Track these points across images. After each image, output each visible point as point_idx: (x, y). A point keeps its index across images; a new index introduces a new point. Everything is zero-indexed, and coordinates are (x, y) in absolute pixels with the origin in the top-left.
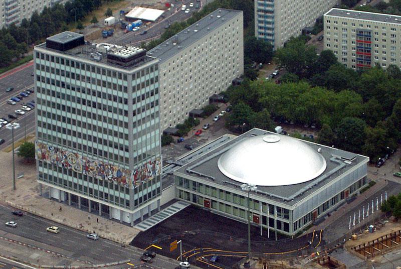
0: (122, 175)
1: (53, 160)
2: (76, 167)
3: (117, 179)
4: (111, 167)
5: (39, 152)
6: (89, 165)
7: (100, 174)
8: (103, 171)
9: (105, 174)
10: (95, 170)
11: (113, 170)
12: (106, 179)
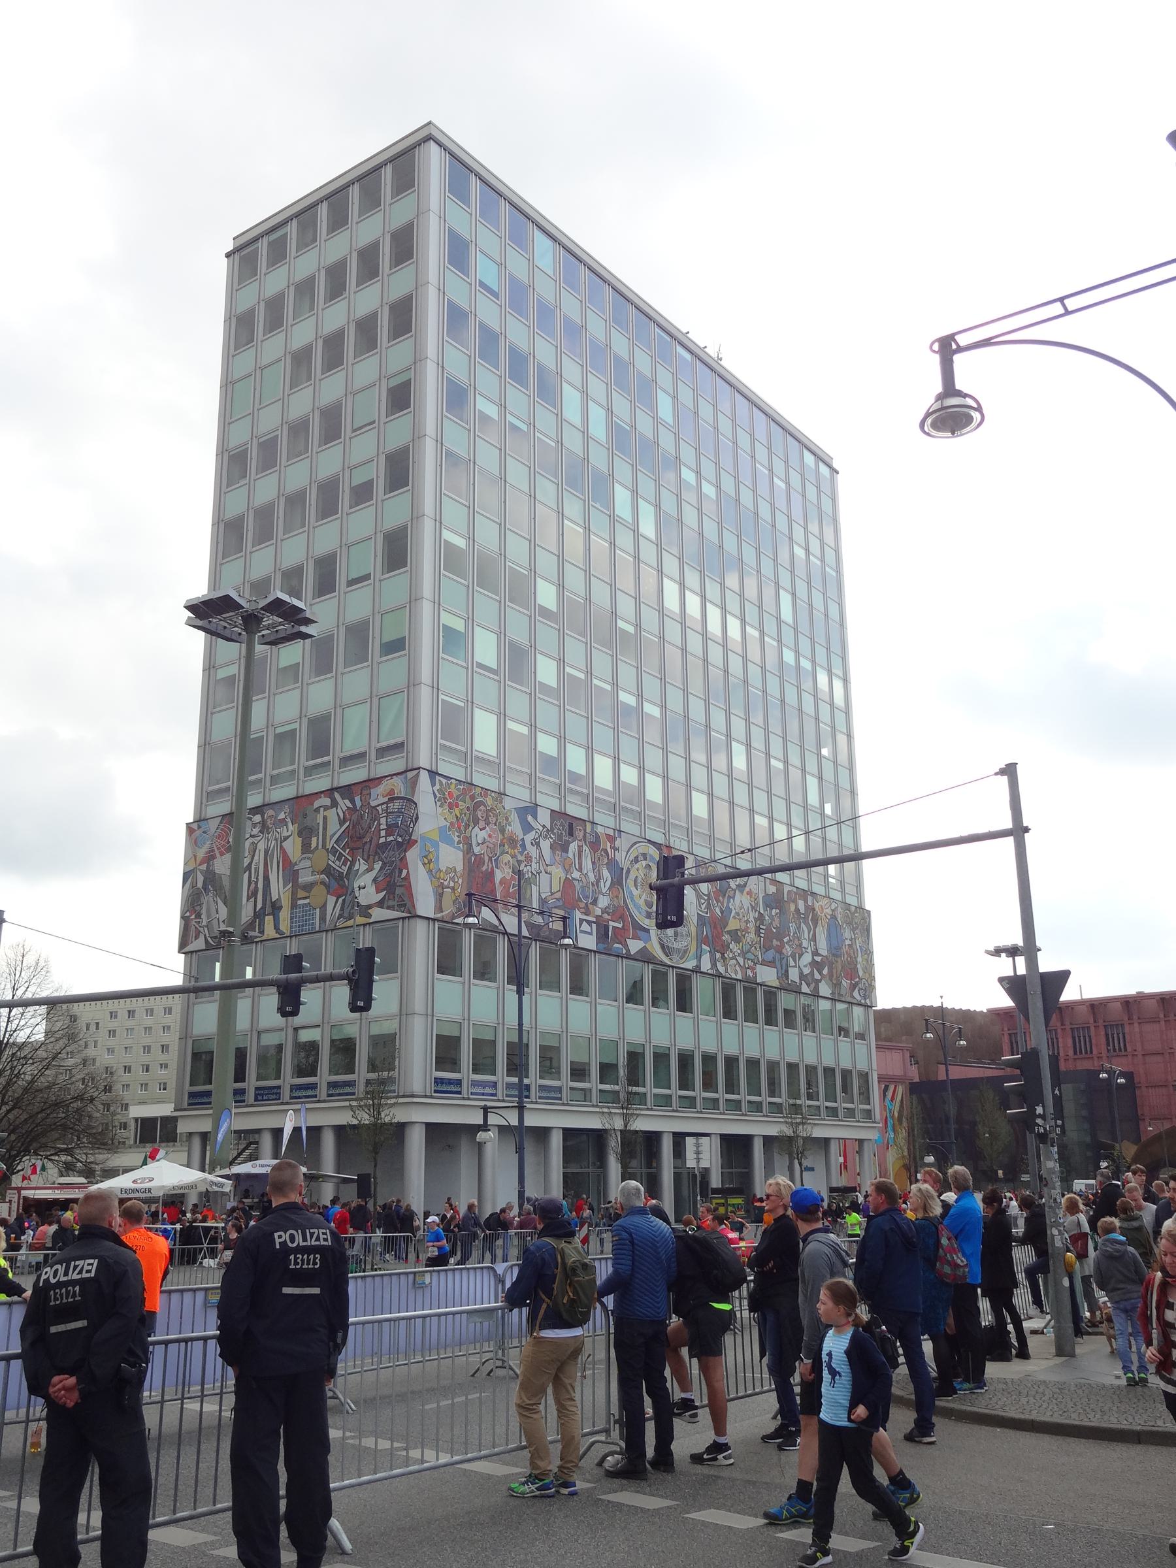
1: (543, 901)
4: (807, 907)
5: (451, 858)
6: (726, 912)
10: (751, 936)
11: (815, 921)
12: (794, 975)
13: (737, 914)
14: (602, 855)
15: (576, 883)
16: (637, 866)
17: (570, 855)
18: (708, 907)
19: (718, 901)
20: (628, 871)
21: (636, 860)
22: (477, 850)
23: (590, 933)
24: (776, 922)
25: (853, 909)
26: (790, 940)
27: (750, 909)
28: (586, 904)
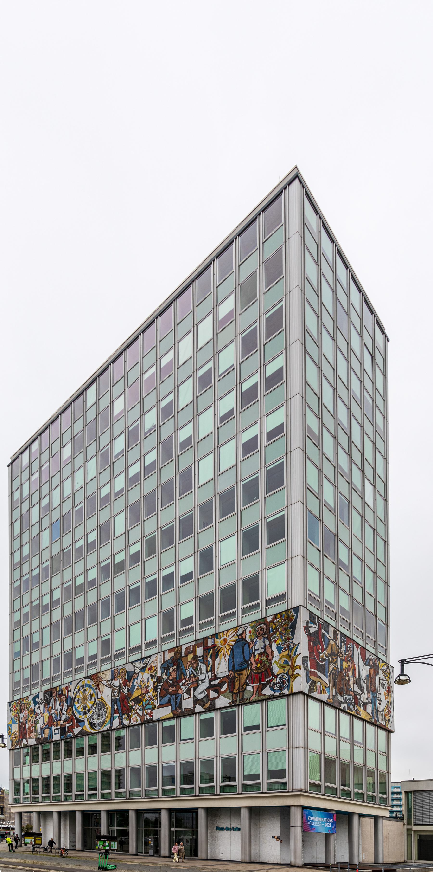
1: (41, 728)
2: (95, 716)
4: (206, 649)
7: (166, 699)
8: (176, 683)
10: (152, 693)
11: (215, 656)
12: (188, 703)
13: (140, 686)
14: (63, 698)
15: (53, 715)
16: (79, 693)
17: (51, 705)
18: (120, 692)
19: (125, 686)
20: (75, 697)
21: (79, 690)
22: (21, 721)
23: (58, 733)
24: (174, 675)
26: (186, 681)
27: (150, 678)
28: (57, 722)
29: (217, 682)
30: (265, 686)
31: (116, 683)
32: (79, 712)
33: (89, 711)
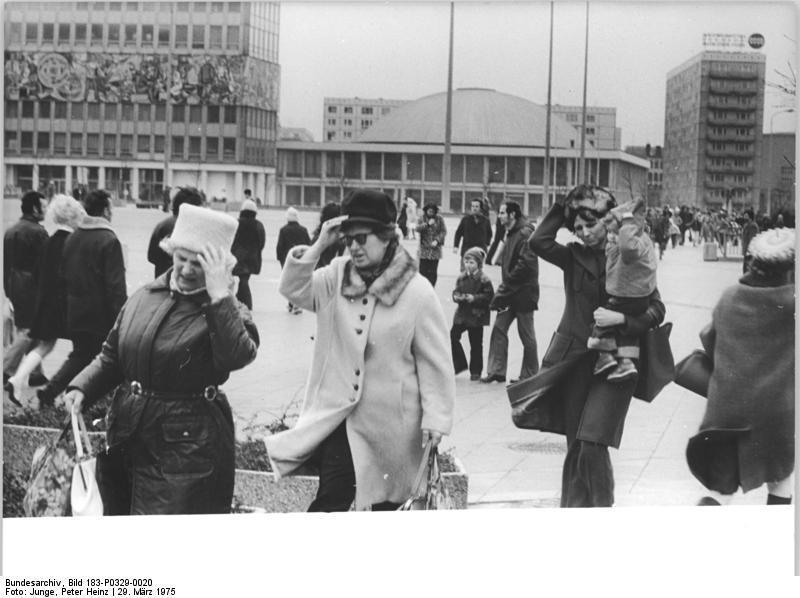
0: (216, 75)
2: (67, 88)
3: (200, 89)
4: (181, 63)
7: (144, 89)
8: (153, 79)
9: (161, 85)
10: (130, 82)
12: (163, 96)
21: (47, 61)
24: (152, 73)
25: (228, 57)
29: (186, 86)
30: (223, 97)
31: (93, 65)
32: (46, 80)
33: (59, 81)
